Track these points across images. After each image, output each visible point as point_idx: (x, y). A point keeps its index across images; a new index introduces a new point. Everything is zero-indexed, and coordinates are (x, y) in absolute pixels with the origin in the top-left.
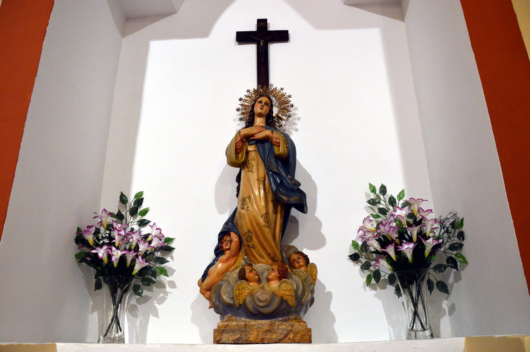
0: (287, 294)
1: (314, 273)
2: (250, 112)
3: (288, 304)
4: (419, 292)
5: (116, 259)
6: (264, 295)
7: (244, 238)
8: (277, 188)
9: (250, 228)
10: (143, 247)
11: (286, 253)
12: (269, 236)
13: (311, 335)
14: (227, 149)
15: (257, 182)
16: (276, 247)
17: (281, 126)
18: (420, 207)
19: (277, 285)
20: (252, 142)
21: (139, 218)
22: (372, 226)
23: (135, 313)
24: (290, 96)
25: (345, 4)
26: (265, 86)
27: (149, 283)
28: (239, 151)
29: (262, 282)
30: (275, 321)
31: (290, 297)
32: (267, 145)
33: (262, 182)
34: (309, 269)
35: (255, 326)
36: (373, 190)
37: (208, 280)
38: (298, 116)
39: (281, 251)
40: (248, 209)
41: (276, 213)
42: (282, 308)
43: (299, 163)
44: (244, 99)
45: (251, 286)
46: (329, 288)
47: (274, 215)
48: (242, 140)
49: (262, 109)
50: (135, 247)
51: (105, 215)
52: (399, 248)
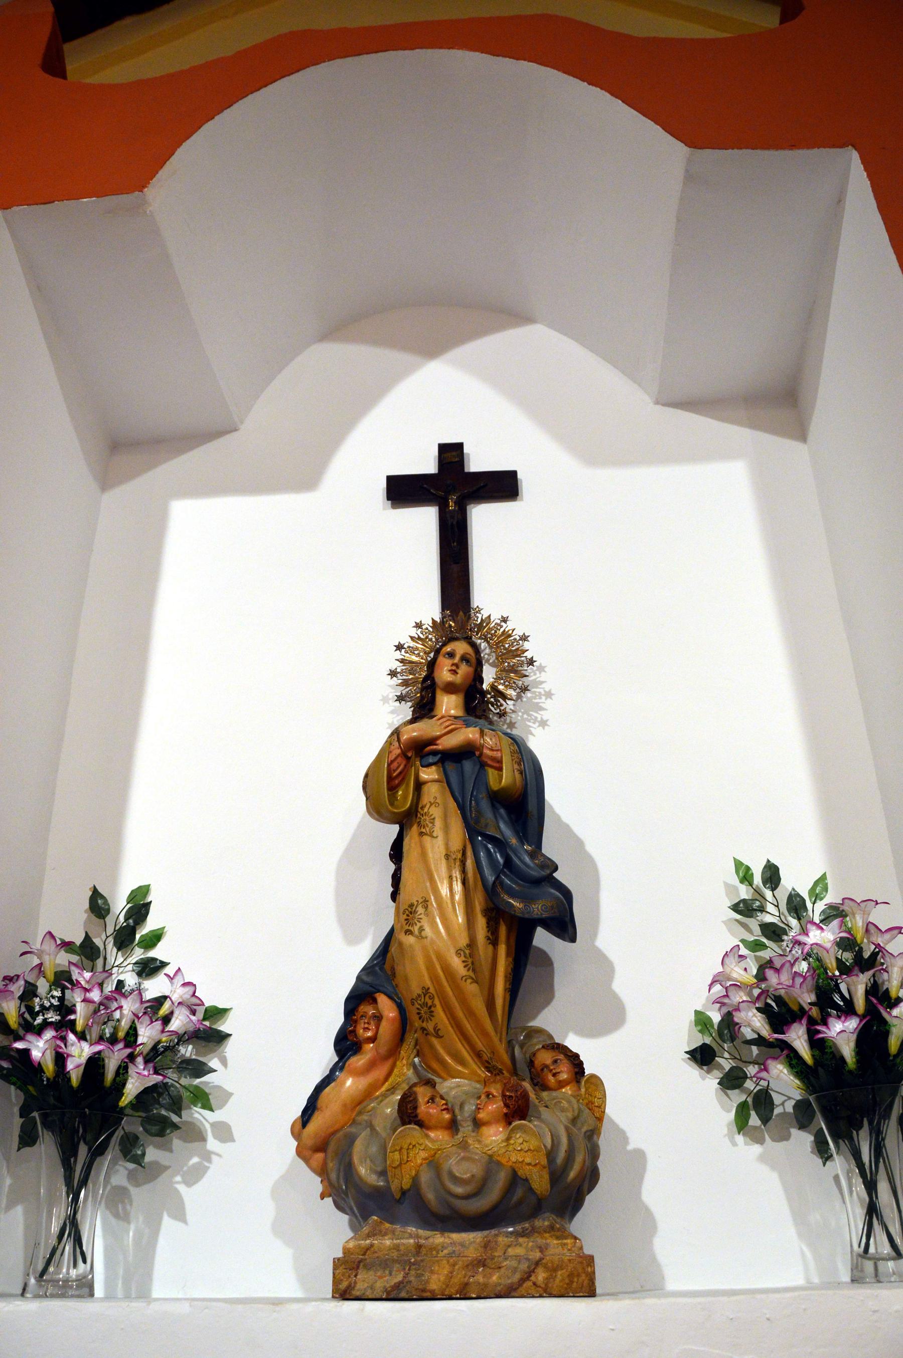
0: (528, 1160)
1: (597, 1102)
2: (425, 679)
3: (531, 1189)
4: (878, 1150)
5: (78, 1066)
6: (465, 1165)
7: (412, 1011)
8: (498, 877)
9: (428, 983)
10: (147, 1034)
11: (522, 1046)
12: (479, 1006)
13: (594, 1273)
14: (366, 776)
15: (444, 861)
16: (496, 1031)
17: (502, 714)
18: (871, 919)
19: (501, 1137)
20: (431, 759)
21: (138, 954)
23: (124, 1209)
24: (524, 638)
25: (657, 403)
26: (461, 613)
28: (397, 782)
29: (461, 1129)
30: (496, 1235)
31: (535, 1170)
32: (468, 765)
33: (458, 863)
34: (583, 1090)
35: (444, 1248)
36: (746, 877)
37: (317, 1123)
38: (546, 687)
39: (510, 1045)
40: (423, 933)
41: (493, 941)
42: (515, 1199)
43: (551, 807)
44: (409, 647)
45: (433, 1141)
47: (491, 947)
48: (404, 754)
49: (454, 672)
50: (127, 1034)
51: (50, 946)
52: (819, 1032)
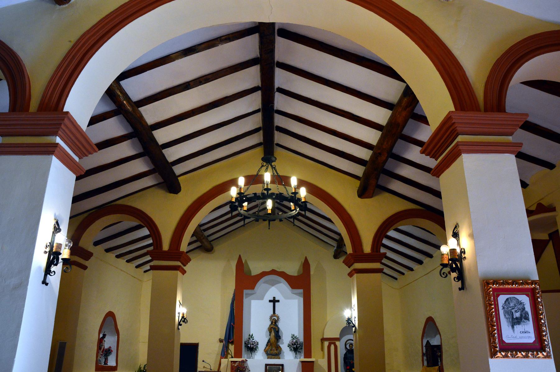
10: (255, 344)
22: (291, 341)
27: (256, 350)
36: (292, 335)
37: (266, 350)
46: (284, 351)
